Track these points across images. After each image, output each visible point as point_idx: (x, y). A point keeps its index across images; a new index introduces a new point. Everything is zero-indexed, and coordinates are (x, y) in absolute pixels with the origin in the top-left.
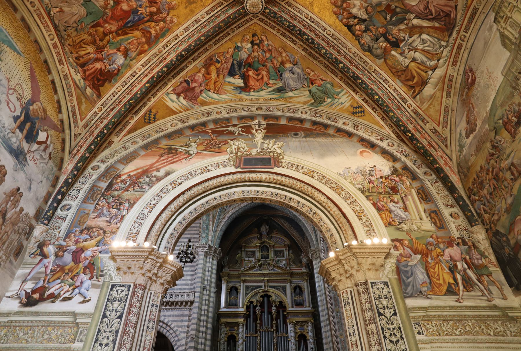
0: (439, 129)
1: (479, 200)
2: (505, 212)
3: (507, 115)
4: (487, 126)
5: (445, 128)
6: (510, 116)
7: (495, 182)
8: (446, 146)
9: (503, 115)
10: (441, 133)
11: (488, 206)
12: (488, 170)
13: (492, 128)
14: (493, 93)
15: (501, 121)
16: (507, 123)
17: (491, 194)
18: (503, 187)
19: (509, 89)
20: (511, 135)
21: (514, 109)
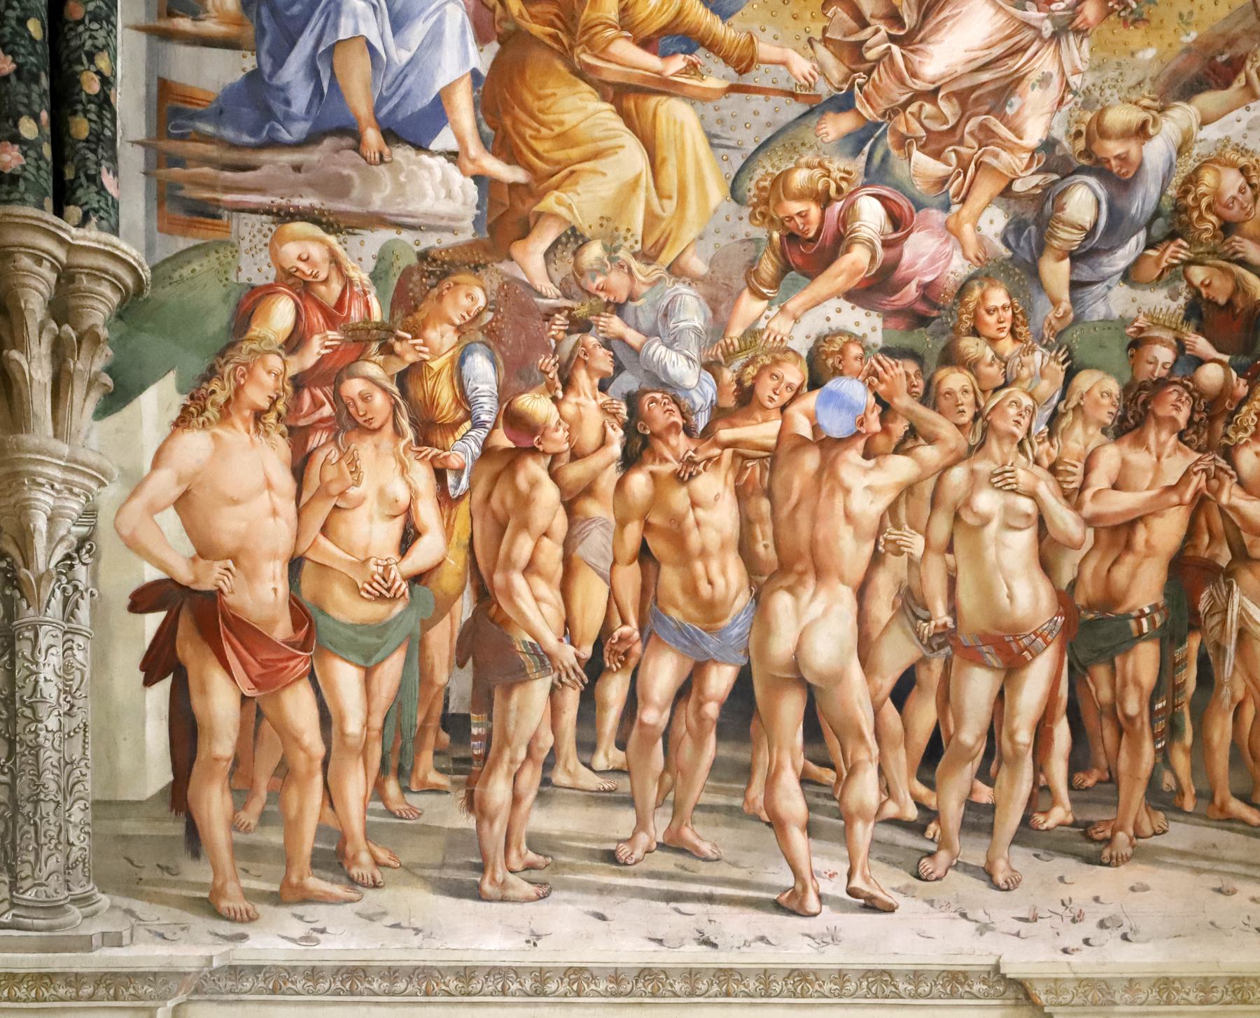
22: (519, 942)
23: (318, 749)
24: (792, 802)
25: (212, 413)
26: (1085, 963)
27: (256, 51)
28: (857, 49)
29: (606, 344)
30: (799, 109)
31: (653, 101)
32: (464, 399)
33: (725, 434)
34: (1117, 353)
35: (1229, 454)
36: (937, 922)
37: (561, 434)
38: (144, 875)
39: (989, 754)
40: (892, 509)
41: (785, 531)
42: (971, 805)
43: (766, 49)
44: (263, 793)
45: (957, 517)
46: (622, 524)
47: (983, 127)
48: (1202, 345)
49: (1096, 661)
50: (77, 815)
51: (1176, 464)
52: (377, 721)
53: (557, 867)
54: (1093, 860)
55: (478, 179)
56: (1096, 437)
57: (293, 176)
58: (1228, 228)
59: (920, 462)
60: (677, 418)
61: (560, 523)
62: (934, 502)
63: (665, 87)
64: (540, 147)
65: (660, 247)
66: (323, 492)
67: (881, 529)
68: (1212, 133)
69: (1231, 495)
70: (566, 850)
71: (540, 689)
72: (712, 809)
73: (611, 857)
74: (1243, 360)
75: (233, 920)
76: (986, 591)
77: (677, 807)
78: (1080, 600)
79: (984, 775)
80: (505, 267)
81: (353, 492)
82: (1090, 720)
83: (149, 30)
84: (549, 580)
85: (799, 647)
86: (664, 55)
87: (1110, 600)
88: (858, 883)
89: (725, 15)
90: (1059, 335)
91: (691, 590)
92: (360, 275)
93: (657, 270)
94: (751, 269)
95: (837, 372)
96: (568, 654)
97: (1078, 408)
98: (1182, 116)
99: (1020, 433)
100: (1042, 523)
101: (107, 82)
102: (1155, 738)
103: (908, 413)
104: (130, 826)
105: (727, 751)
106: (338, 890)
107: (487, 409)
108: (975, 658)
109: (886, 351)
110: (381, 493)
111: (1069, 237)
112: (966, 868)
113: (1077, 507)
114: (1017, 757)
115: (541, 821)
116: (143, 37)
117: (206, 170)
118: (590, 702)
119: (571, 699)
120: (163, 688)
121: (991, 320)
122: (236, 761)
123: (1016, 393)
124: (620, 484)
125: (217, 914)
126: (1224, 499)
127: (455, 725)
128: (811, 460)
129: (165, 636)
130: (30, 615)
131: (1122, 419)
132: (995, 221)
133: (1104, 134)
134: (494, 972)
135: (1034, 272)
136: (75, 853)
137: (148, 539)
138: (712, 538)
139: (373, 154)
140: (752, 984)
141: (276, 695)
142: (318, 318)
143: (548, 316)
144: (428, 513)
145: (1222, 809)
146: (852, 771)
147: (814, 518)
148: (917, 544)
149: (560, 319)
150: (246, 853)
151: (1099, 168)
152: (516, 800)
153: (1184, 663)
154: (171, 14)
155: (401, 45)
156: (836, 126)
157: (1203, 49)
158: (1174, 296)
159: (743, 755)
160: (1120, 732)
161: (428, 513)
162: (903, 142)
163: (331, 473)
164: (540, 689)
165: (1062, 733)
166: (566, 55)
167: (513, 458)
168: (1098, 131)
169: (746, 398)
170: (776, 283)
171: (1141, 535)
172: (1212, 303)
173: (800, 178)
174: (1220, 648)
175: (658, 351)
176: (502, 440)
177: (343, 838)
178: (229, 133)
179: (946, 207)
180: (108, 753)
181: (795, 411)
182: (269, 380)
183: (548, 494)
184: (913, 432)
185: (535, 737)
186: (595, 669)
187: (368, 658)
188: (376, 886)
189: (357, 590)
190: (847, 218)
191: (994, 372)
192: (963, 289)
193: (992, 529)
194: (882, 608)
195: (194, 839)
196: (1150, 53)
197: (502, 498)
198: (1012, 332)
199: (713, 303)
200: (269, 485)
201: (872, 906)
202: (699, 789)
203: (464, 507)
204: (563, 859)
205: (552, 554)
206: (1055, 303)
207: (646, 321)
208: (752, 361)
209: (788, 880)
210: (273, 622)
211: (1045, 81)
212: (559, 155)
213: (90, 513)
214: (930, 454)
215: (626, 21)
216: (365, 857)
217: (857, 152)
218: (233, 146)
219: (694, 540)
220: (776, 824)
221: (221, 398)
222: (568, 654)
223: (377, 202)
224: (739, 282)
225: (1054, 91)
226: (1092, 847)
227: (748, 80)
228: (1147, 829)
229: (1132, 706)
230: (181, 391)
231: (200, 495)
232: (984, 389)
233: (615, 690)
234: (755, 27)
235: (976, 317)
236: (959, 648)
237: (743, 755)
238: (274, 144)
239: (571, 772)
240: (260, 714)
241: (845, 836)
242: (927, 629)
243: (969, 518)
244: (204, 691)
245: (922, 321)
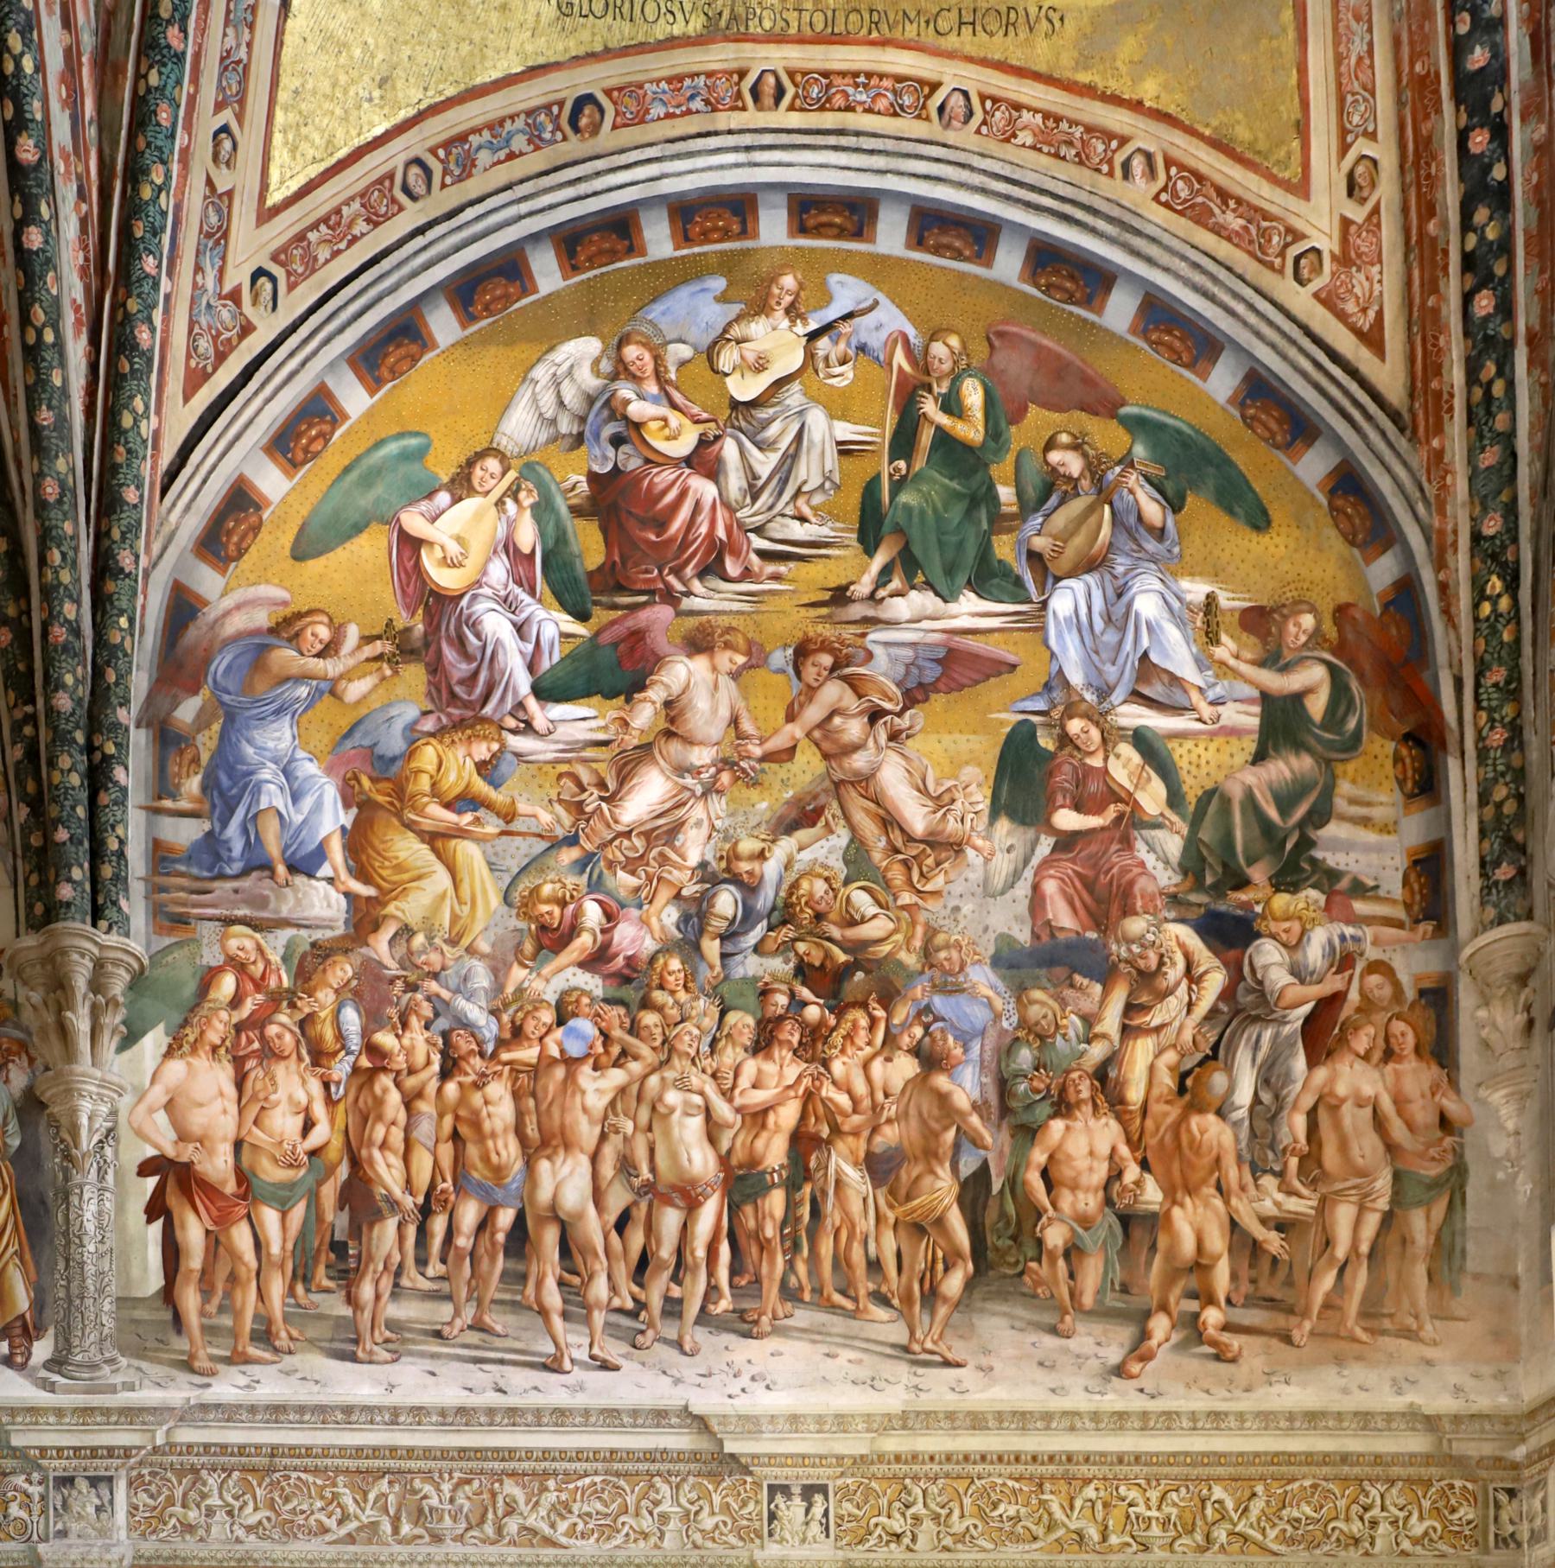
22: (381, 1390)
23: (254, 1264)
24: (553, 1298)
25: (186, 1048)
26: (743, 1404)
27: (210, 818)
28: (579, 807)
29: (428, 999)
30: (544, 845)
31: (453, 842)
32: (340, 1036)
33: (505, 1056)
34: (752, 1000)
35: (826, 1064)
36: (649, 1378)
37: (401, 1058)
39: (679, 1265)
40: (612, 1104)
41: (544, 1119)
42: (668, 1299)
43: (522, 807)
44: (220, 1293)
45: (654, 1109)
46: (441, 1116)
47: (661, 854)
48: (806, 993)
49: (744, 1202)
50: (107, 1307)
51: (792, 1071)
52: (290, 1246)
53: (404, 1341)
54: (747, 1335)
55: (347, 894)
56: (741, 1054)
57: (233, 896)
58: (819, 917)
59: (629, 1072)
60: (474, 1047)
61: (402, 1116)
62: (639, 1098)
63: (461, 833)
64: (384, 873)
65: (460, 936)
66: (254, 1097)
67: (605, 1117)
68: (806, 856)
69: (828, 1091)
70: (410, 1330)
71: (391, 1224)
72: (501, 1302)
73: (438, 1334)
74: (832, 1002)
75: (201, 1374)
76: (674, 1156)
77: (480, 1302)
78: (734, 1162)
79: (676, 1279)
80: (364, 950)
81: (273, 1097)
82: (742, 1241)
83: (147, 808)
84: (395, 1153)
85: (555, 1196)
86: (460, 812)
87: (753, 1162)
88: (596, 1351)
89: (496, 786)
90: (715, 988)
91: (486, 1159)
92: (275, 958)
93: (459, 951)
94: (518, 949)
95: (575, 1015)
96: (408, 1202)
97: (729, 1035)
98: (786, 845)
99: (692, 1052)
100: (708, 1112)
101: (122, 842)
102: (784, 1253)
103: (620, 1041)
104: (140, 1314)
105: (511, 1265)
106: (267, 1355)
107: (355, 1042)
108: (668, 1201)
109: (606, 1001)
110: (290, 1098)
111: (718, 925)
112: (666, 1341)
113: (730, 1100)
114: (696, 1267)
115: (393, 1310)
116: (143, 814)
117: (182, 894)
118: (423, 1233)
119: (411, 1231)
120: (158, 1226)
121: (671, 979)
122: (204, 1272)
123: (688, 1026)
124: (440, 1090)
125: (193, 1371)
126: (824, 1093)
127: (339, 1248)
128: (560, 1072)
129: (159, 1191)
130: (77, 1179)
131: (757, 1042)
132: (671, 915)
133: (738, 858)
134: (366, 1409)
135: (697, 947)
137: (148, 1129)
138: (498, 1125)
139: (282, 880)
140: (530, 1418)
141: (227, 1230)
142: (250, 986)
143: (392, 981)
144: (319, 1110)
145: (829, 1299)
146: (591, 1277)
147: (563, 1110)
148: (629, 1127)
149: (399, 984)
150: (210, 1331)
151: (736, 880)
152: (378, 1297)
153: (801, 1202)
155: (298, 811)
156: (569, 855)
157: (797, 802)
158: (787, 962)
159: (521, 1267)
160: (762, 1249)
161: (319, 1110)
162: (611, 865)
163: (259, 1086)
164: (391, 1224)
165: (725, 1250)
166: (399, 814)
167: (372, 1074)
168: (733, 856)
169: (517, 1033)
170: (534, 958)
171: (771, 1118)
172: (811, 965)
173: (547, 890)
174: (824, 1193)
175: (461, 1003)
176: (365, 1063)
177: (269, 1322)
178: (195, 871)
179: (640, 907)
180: (124, 1270)
181: (549, 1040)
182: (220, 1027)
183: (394, 1097)
184: (624, 1053)
185: (388, 1257)
186: (426, 1211)
187: (283, 1204)
188: (290, 1353)
189: (276, 1161)
190: (578, 914)
191: (674, 1013)
192: (652, 960)
193: (676, 1116)
194: (608, 1169)
195: (178, 1321)
196: (764, 805)
197: (365, 1100)
198: (685, 987)
199: (495, 971)
200: (222, 1094)
201: (606, 1366)
202: (493, 1290)
203: (341, 1107)
204: (408, 1335)
205: (397, 1136)
206: (712, 967)
207: (453, 983)
208: (520, 1008)
209: (551, 1349)
210: (224, 1182)
211: (699, 824)
212: (396, 878)
213: (114, 1113)
214: (635, 1067)
215: (435, 792)
216: (283, 1334)
217: (582, 872)
218: (197, 879)
219: (487, 1126)
220: (543, 1312)
221: (191, 1038)
222: (408, 1202)
223: (285, 911)
224: (511, 958)
225: (705, 830)
226: (746, 1326)
227: (515, 827)
228: (780, 1314)
229: (770, 1231)
231: (181, 1101)
232: (668, 1024)
233: (439, 1225)
234: (516, 794)
235: (661, 977)
236: (657, 1194)
237: (521, 1267)
238: (222, 876)
239: (412, 1278)
240: (217, 1242)
241: (587, 1320)
242: (637, 1182)
243: (662, 1109)
244: (183, 1227)
245: (627, 980)
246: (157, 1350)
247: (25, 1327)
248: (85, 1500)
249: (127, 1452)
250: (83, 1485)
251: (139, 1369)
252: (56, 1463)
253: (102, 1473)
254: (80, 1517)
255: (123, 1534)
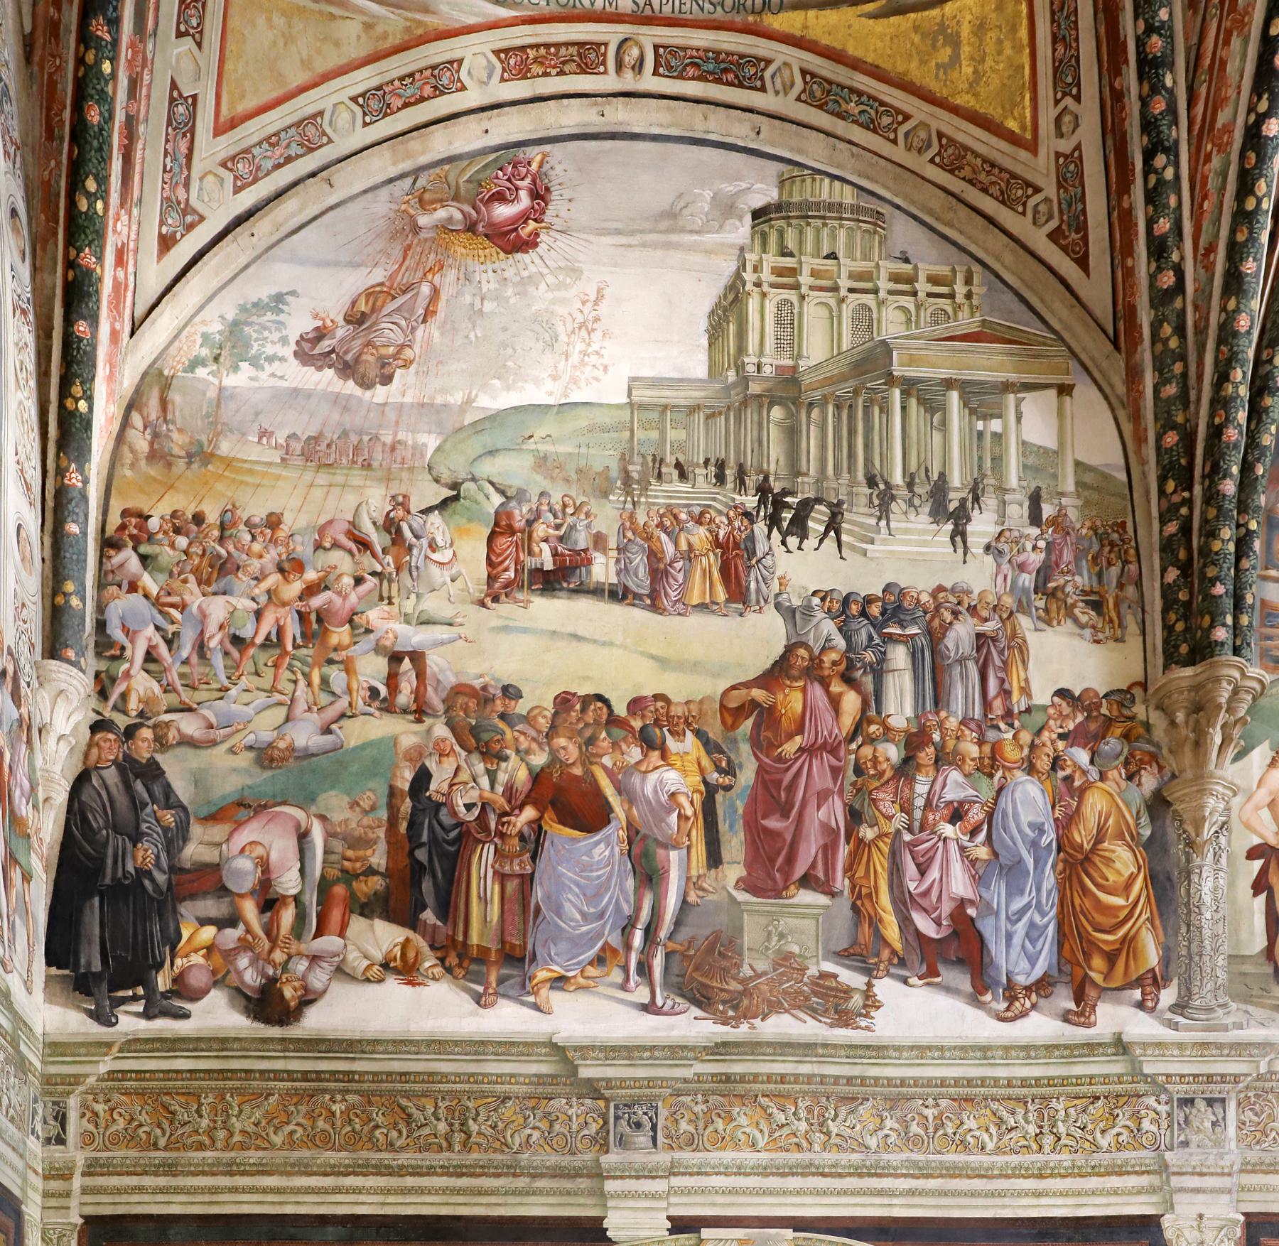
0: (210, 149)
1: (157, 603)
2: (250, 748)
3: (538, 515)
4: (431, 442)
5: (229, 177)
6: (540, 530)
7: (292, 628)
8: (166, 243)
9: (521, 495)
10: (198, 167)
11: (186, 662)
12: (299, 566)
13: (446, 477)
14: (549, 385)
15: (497, 500)
16: (512, 531)
17: (237, 640)
18: (316, 679)
19: (605, 458)
20: (491, 579)
21: (572, 528)
38: (1254, 993)
50: (1221, 961)
104: (1247, 968)
120: (1263, 897)
129: (1264, 871)
130: (1197, 861)
136: (1220, 982)
137: (1255, 823)
154: (1267, 568)
213: (1227, 809)
230: (1272, 749)
246: (1259, 997)
247: (1155, 978)
248: (1203, 1116)
249: (1236, 1079)
250: (1201, 1104)
251: (1247, 1012)
252: (1179, 1087)
253: (1217, 1095)
254: (1199, 1130)
255: (1233, 1144)
